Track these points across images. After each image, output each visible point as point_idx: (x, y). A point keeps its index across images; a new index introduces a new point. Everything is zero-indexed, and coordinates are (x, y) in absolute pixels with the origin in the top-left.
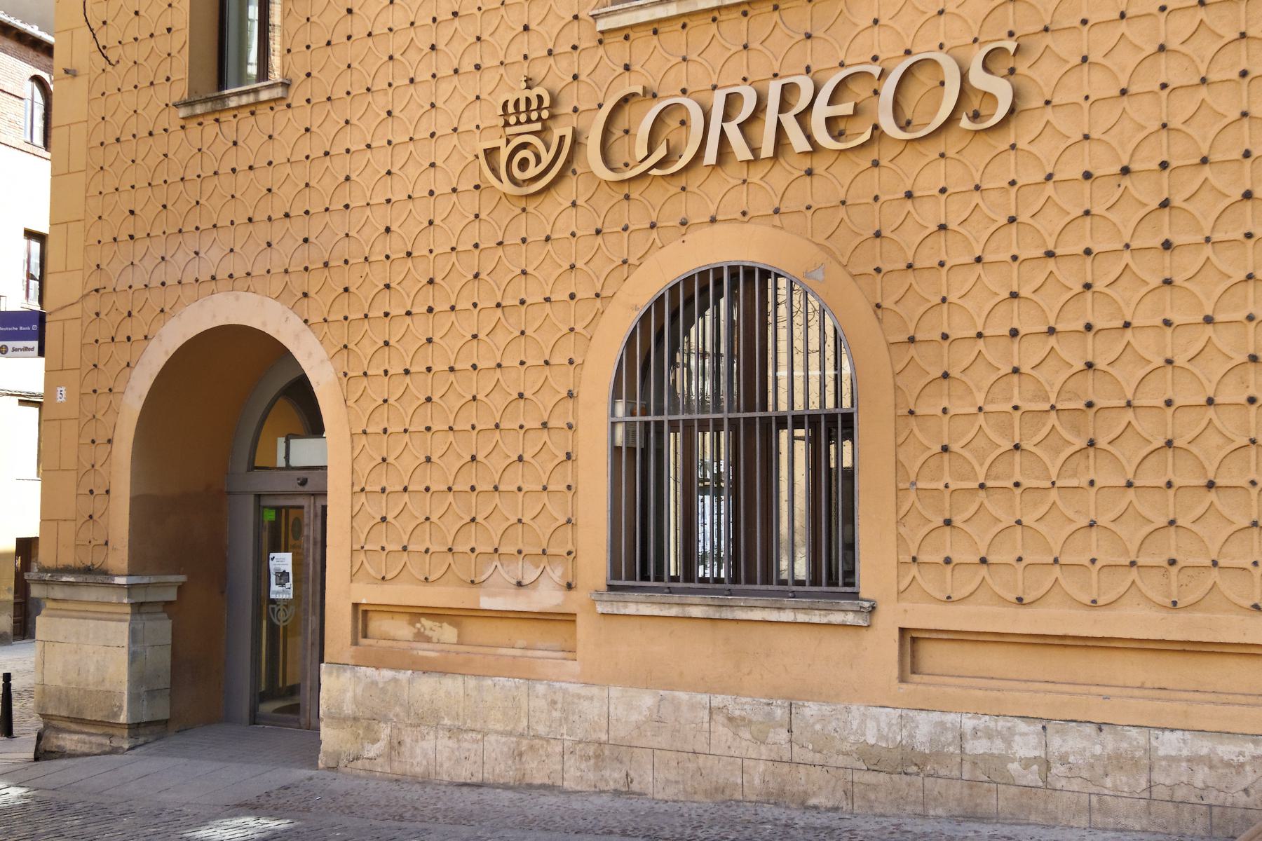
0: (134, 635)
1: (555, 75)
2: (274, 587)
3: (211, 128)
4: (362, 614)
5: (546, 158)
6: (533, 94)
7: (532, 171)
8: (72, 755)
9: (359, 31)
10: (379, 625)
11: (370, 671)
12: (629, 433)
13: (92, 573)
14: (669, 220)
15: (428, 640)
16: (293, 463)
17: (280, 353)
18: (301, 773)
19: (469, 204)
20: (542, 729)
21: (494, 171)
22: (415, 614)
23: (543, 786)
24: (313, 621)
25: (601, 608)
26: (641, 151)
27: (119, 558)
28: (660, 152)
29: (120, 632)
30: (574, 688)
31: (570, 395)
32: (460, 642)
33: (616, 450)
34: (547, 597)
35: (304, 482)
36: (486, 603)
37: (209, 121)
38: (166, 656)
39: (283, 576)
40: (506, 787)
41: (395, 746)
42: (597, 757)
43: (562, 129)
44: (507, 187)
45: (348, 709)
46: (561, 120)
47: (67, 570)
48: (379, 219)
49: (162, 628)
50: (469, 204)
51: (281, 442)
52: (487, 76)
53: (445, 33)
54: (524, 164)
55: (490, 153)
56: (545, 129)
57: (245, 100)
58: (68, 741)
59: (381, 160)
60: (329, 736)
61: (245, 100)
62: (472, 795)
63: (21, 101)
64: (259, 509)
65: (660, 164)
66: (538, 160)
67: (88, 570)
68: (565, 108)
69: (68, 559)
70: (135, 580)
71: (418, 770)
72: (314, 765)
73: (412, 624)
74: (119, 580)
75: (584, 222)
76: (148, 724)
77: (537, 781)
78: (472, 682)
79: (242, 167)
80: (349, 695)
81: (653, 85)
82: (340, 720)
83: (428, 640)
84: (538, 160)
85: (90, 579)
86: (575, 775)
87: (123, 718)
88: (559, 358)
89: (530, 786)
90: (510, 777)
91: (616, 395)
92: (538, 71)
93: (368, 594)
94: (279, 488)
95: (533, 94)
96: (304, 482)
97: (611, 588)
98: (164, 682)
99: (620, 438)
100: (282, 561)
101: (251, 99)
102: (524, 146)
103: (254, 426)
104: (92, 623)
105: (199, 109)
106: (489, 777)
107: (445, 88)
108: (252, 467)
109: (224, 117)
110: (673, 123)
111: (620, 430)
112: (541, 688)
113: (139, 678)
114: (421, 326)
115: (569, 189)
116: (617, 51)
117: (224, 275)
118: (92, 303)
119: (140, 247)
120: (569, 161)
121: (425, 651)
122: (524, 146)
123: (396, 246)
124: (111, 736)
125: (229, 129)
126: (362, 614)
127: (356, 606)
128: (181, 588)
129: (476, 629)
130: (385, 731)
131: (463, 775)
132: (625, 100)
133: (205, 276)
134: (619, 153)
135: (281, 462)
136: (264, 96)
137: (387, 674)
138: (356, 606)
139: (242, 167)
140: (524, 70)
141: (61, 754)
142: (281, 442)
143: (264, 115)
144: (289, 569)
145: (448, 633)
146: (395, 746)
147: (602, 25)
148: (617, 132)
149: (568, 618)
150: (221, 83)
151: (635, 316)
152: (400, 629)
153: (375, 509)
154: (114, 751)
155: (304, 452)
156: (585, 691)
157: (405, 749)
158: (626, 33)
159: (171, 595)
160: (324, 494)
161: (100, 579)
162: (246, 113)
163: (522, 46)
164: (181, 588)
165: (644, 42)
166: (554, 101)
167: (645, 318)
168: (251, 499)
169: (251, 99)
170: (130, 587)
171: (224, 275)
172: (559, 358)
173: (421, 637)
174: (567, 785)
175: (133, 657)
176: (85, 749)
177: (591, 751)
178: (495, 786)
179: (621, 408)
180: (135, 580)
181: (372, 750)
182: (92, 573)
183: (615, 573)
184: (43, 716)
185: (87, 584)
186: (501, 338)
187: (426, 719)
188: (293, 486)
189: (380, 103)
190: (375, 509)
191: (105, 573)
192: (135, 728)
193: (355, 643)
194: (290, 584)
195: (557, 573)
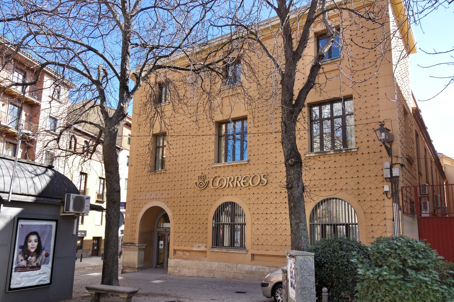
0: (138, 253)
1: (206, 173)
2: (160, 246)
3: (154, 176)
4: (175, 251)
5: (204, 185)
6: (202, 175)
7: (202, 186)
8: (128, 273)
9: (177, 163)
10: (177, 252)
11: (176, 259)
12: (215, 225)
13: (132, 244)
14: (221, 195)
15: (185, 255)
16: (164, 227)
17: (161, 210)
18: (165, 275)
19: (193, 190)
20: (201, 268)
21: (197, 186)
22: (183, 251)
23: (201, 277)
24: (166, 252)
25: (210, 250)
26: (218, 184)
27: (137, 241)
28: (220, 185)
29: (136, 253)
30: (206, 262)
31: (207, 219)
32: (190, 255)
33: (213, 227)
34: (203, 249)
35: (166, 230)
36: (194, 249)
37: (154, 174)
38: (143, 257)
39: (162, 245)
40: (196, 277)
41: (180, 271)
42: (209, 272)
43: (206, 181)
44: (198, 188)
45: (173, 265)
46: (206, 179)
47: (128, 243)
48: (179, 191)
49: (143, 253)
50: (193, 190)
51: (162, 223)
52: (196, 172)
53: (190, 165)
54: (201, 185)
55: (196, 183)
56: (204, 180)
57: (159, 172)
58: (127, 270)
59: (180, 183)
60: (169, 269)
61: (159, 172)
62: (191, 278)
63: (237, 291)
64: (158, 234)
65: (220, 187)
66: (203, 185)
67: (131, 243)
68: (207, 177)
69: (128, 241)
70: (139, 245)
71: (183, 274)
72: (167, 273)
73: (183, 252)
74: (137, 245)
75: (209, 194)
76: (140, 268)
77: (201, 276)
78: (191, 261)
79: (159, 182)
80: (173, 263)
81: (220, 175)
82: (171, 267)
83: (185, 255)
84: (203, 185)
85: (132, 245)
86: (206, 275)
87: (136, 267)
88: (205, 214)
89: (200, 277)
90: (197, 275)
91: (213, 219)
92: (203, 172)
93: (176, 248)
94: (161, 231)
95: (202, 175)
96: (166, 230)
97: (212, 247)
98: (143, 261)
99: (214, 226)
100: (162, 242)
101: (160, 172)
102: (201, 182)
103: (158, 220)
104: (132, 252)
105: (152, 173)
106: (194, 276)
107: (190, 173)
108: (157, 227)
109: (156, 174)
110: (222, 181)
111: (214, 224)
112: (201, 262)
113: (139, 260)
114: (185, 208)
115: (207, 189)
116: (215, 170)
117: (155, 198)
118: (134, 201)
119: (142, 193)
120: (207, 185)
121: (184, 256)
122: (201, 182)
123: (182, 196)
124: (134, 270)
125: (157, 176)
126: (175, 251)
127: (174, 249)
128: (146, 246)
129: (192, 253)
130: (178, 269)
131: (190, 275)
132: (216, 177)
133: (152, 198)
134: (214, 185)
135: (162, 227)
136: (162, 172)
137: (179, 260)
138: (174, 249)
139: (159, 182)
140: (201, 171)
141: (126, 272)
142: (162, 223)
143: (162, 174)
144: (163, 244)
145: (188, 254)
146: (180, 271)
147: (213, 166)
148: (214, 182)
149: (206, 252)
150: (155, 170)
151: (216, 208)
152: (181, 253)
153: (177, 235)
154: (135, 272)
155: (166, 225)
156: (208, 262)
157: (181, 271)
158: (216, 168)
159: (144, 247)
160: (170, 232)
161: (134, 245)
162: (159, 174)
163: (201, 168)
164: (146, 246)
165: (218, 169)
166: (206, 176)
167: (218, 208)
168: (157, 233)
169: (160, 172)
170: (138, 246)
171: (155, 198)
172: (205, 214)
173: (184, 254)
174: (205, 276)
175: (138, 257)
176: (130, 272)
177: (209, 271)
178: (194, 277)
179: (214, 221)
180: (139, 245)
181: (176, 272)
182: (132, 244)
183: (213, 245)
184: (123, 266)
185: (131, 245)
186: (197, 210)
187: (185, 267)
188: (164, 231)
189: (180, 174)
190: (177, 235)
191: (134, 244)
192: (138, 268)
193: (174, 255)
194: (163, 246)
195: (204, 245)
